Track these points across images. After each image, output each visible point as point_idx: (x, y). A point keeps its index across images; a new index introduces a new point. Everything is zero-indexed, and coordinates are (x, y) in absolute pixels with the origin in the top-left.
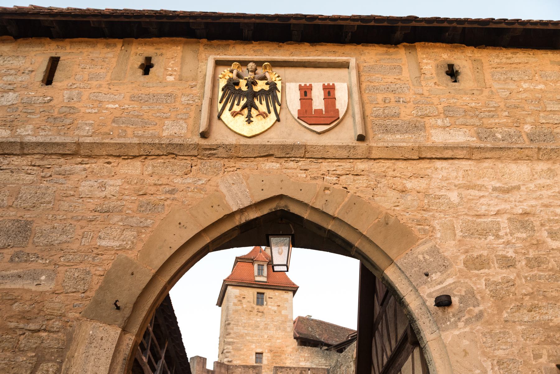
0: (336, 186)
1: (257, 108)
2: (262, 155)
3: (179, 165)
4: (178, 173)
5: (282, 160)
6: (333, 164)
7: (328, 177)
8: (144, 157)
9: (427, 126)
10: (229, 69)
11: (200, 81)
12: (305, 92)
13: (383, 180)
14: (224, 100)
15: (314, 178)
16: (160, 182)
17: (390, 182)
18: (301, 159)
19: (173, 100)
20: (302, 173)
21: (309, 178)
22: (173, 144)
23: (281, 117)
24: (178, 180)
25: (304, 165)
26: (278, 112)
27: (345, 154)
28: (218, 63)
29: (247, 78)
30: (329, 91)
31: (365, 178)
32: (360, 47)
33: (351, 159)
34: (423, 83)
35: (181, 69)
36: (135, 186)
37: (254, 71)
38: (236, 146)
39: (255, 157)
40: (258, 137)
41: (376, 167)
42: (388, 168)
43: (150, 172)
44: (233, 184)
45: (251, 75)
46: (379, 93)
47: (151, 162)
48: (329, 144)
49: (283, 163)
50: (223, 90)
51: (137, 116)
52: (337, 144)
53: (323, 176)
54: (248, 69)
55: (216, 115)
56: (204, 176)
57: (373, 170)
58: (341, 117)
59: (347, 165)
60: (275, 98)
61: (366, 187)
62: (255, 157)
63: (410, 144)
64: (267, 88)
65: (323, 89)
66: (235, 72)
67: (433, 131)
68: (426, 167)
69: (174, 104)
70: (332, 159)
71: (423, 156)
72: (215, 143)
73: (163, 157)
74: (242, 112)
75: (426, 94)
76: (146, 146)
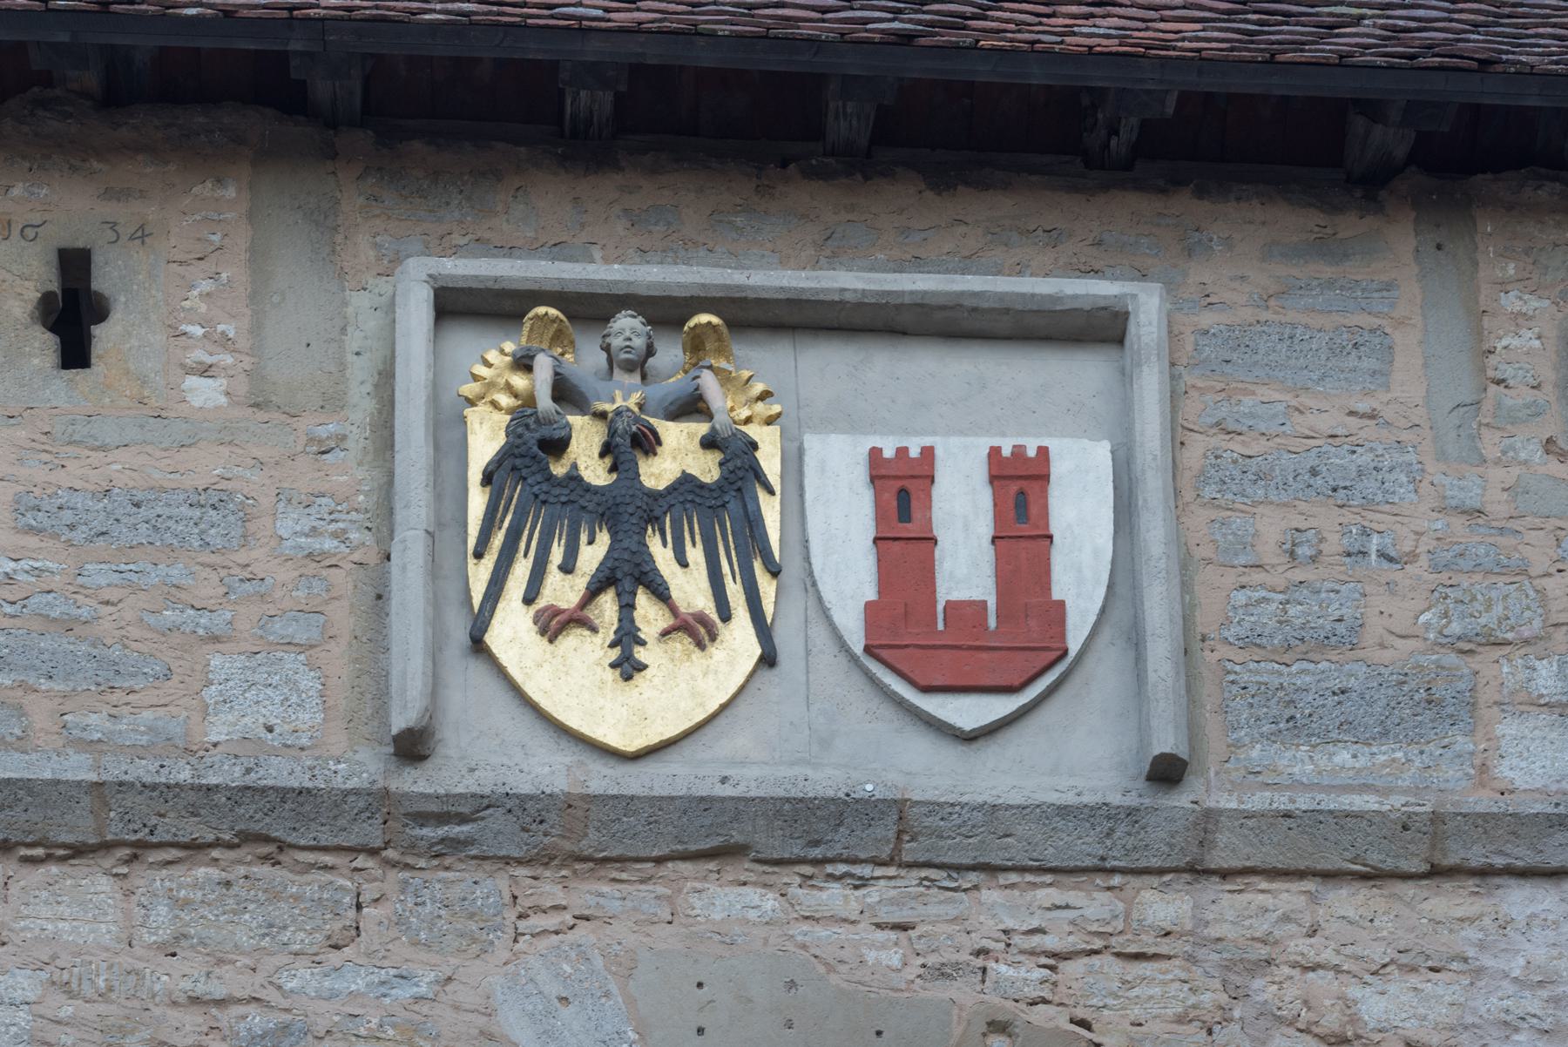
0: (1040, 1014)
1: (661, 594)
2: (693, 847)
3: (297, 898)
4: (298, 938)
5: (789, 876)
6: (1029, 895)
7: (1003, 968)
8: (125, 852)
9: (1486, 695)
10: (509, 347)
11: (362, 405)
12: (901, 489)
13: (1258, 983)
14: (498, 540)
15: (942, 973)
16: (219, 992)
17: (1291, 992)
18: (879, 872)
19: (236, 532)
20: (883, 947)
21: (913, 971)
22: (263, 790)
23: (781, 638)
24: (301, 978)
25: (892, 902)
26: (768, 608)
27: (1084, 846)
28: (455, 307)
29: (609, 407)
30: (1020, 484)
31: (1175, 969)
32: (1184, 204)
33: (1114, 871)
34: (1491, 444)
35: (256, 329)
36: (102, 1008)
37: (639, 365)
38: (573, 806)
39: (659, 861)
40: (672, 754)
41: (1230, 915)
42: (1286, 918)
43: (165, 934)
44: (564, 1000)
45: (625, 396)
46: (1265, 502)
47: (160, 880)
48: (1016, 799)
49: (794, 891)
50: (487, 479)
51: (68, 626)
52: (1053, 798)
53: (979, 962)
54: (607, 348)
55: (459, 634)
56: (423, 955)
57: (1213, 932)
58: (1074, 646)
59: (1095, 904)
60: (752, 525)
61: (1181, 1020)
62: (659, 861)
63: (1397, 801)
64: (707, 468)
65: (994, 479)
66: (544, 366)
67: (1507, 729)
68: (1459, 913)
69: (242, 557)
70: (1023, 870)
71: (1451, 860)
72: (466, 785)
73: (215, 853)
74: (591, 613)
75: (1498, 504)
76: (130, 800)
